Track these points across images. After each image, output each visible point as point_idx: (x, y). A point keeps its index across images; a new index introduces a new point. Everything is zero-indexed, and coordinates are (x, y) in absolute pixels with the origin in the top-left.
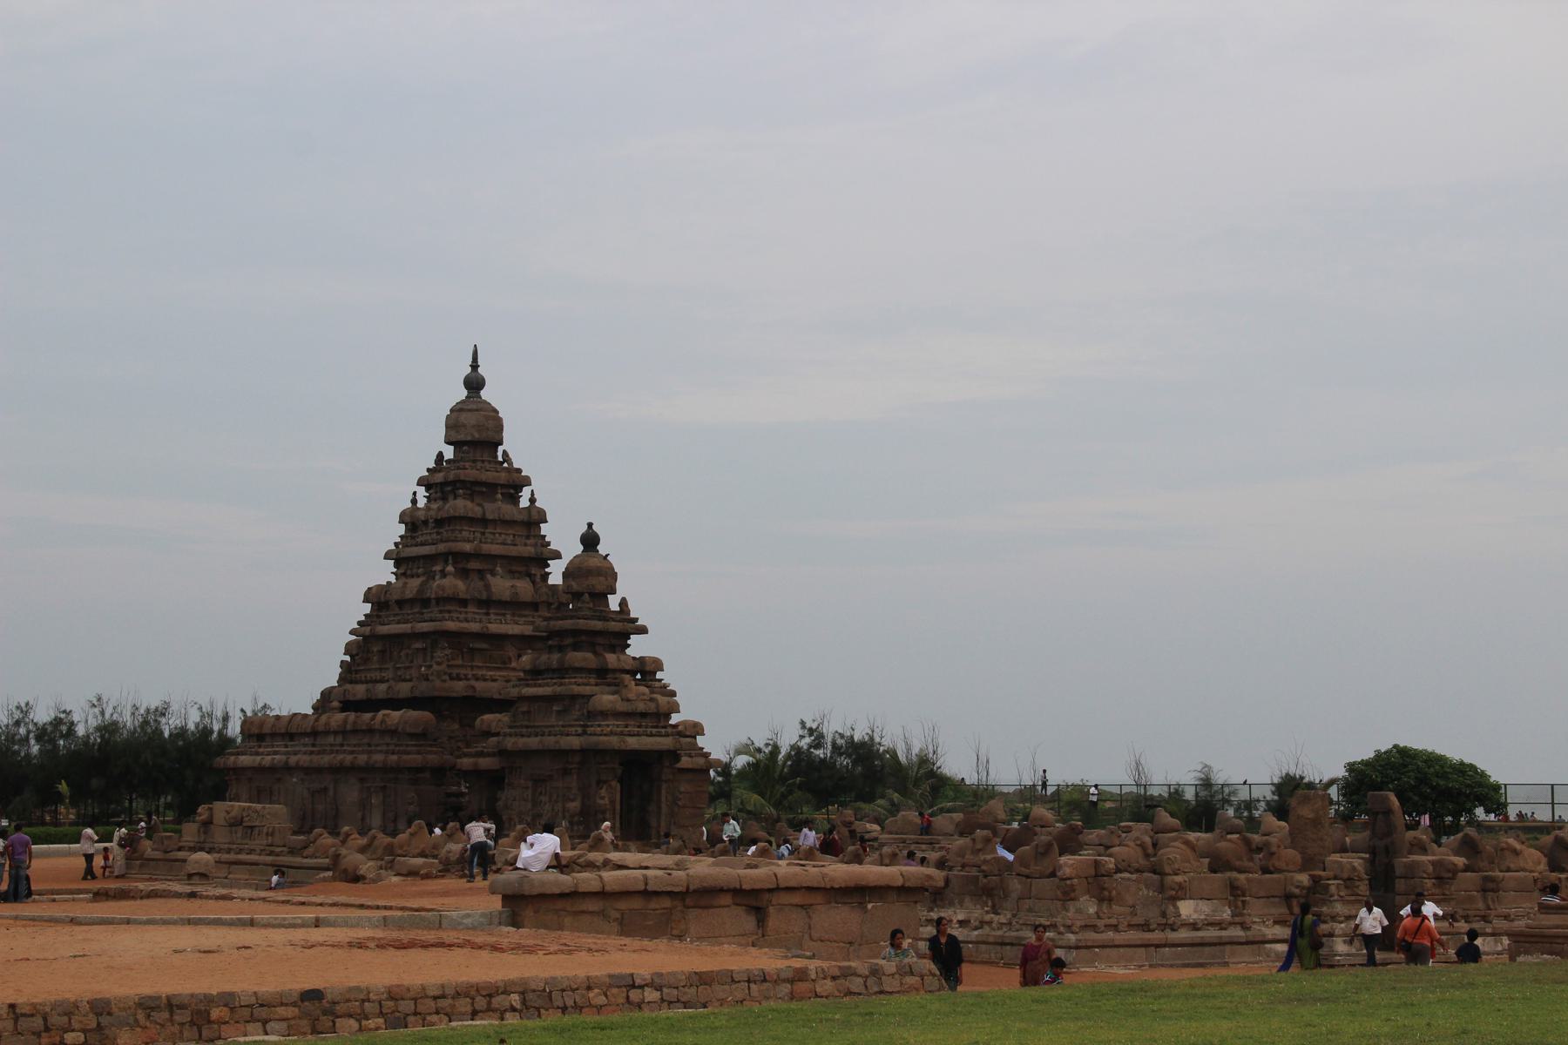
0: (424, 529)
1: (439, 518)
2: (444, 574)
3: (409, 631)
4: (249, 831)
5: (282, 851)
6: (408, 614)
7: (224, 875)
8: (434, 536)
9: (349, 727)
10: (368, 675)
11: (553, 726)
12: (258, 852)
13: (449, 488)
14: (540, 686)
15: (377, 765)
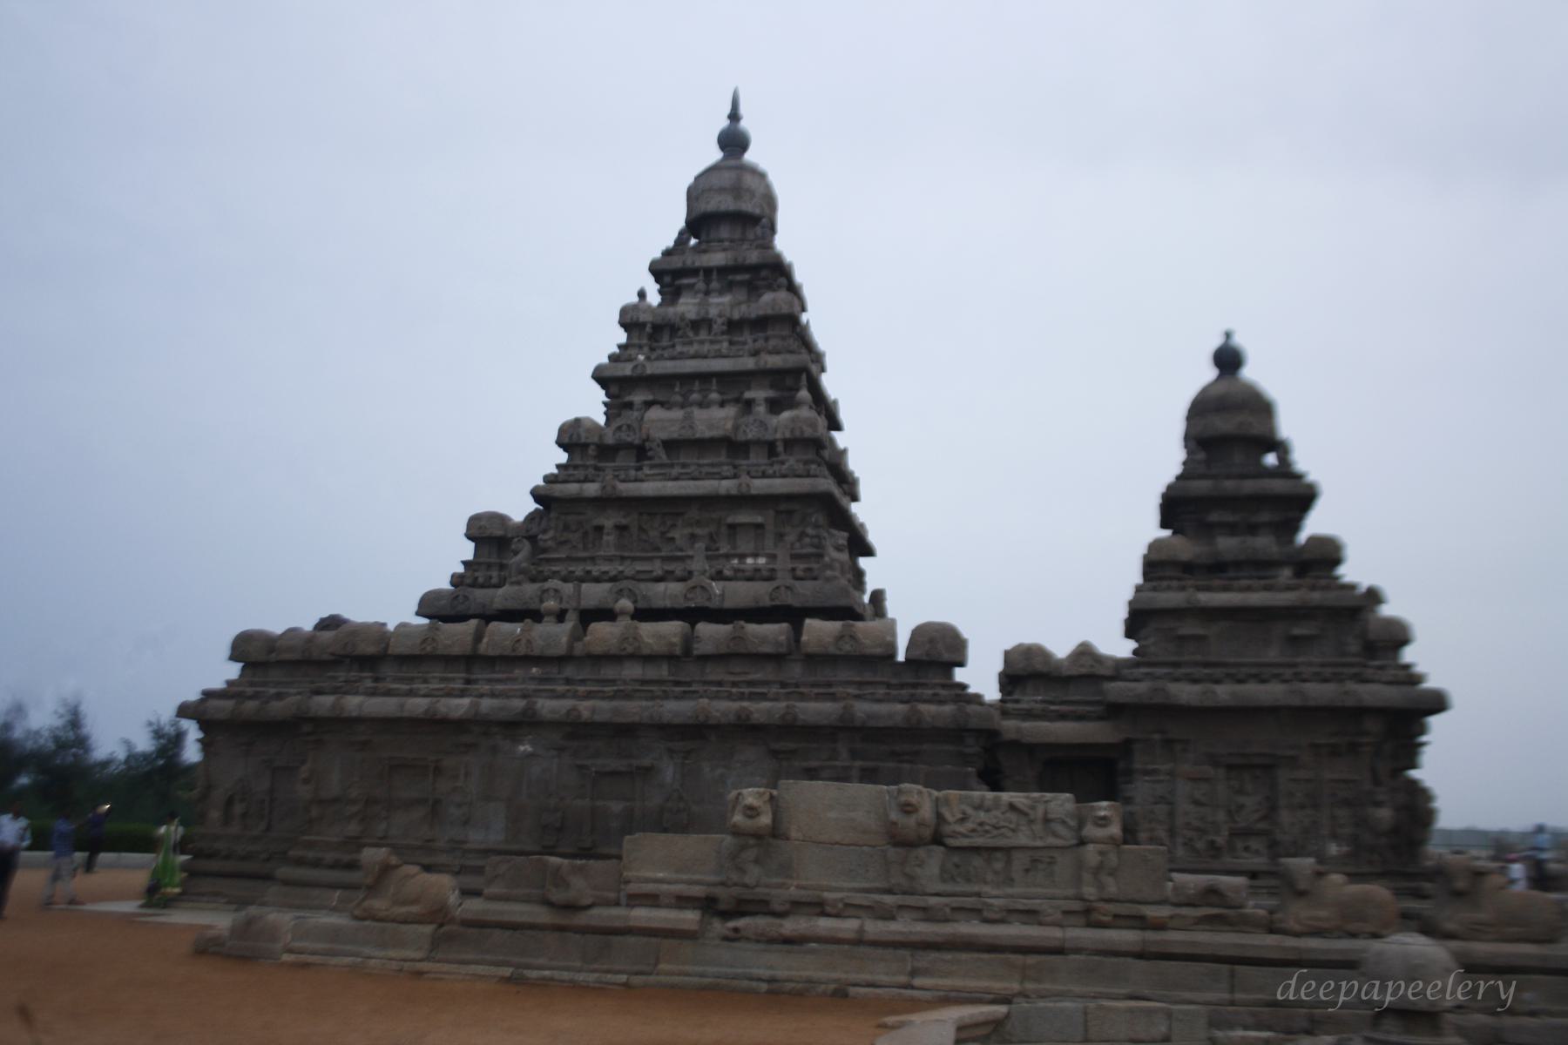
0: (691, 334)
1: (736, 316)
2: (775, 406)
3: (734, 492)
4: (977, 862)
5: (1171, 917)
6: (699, 465)
7: (903, 979)
8: (725, 345)
9: (700, 649)
10: (595, 570)
11: (1294, 665)
12: (1058, 916)
13: (739, 277)
14: (1248, 589)
15: (872, 723)
